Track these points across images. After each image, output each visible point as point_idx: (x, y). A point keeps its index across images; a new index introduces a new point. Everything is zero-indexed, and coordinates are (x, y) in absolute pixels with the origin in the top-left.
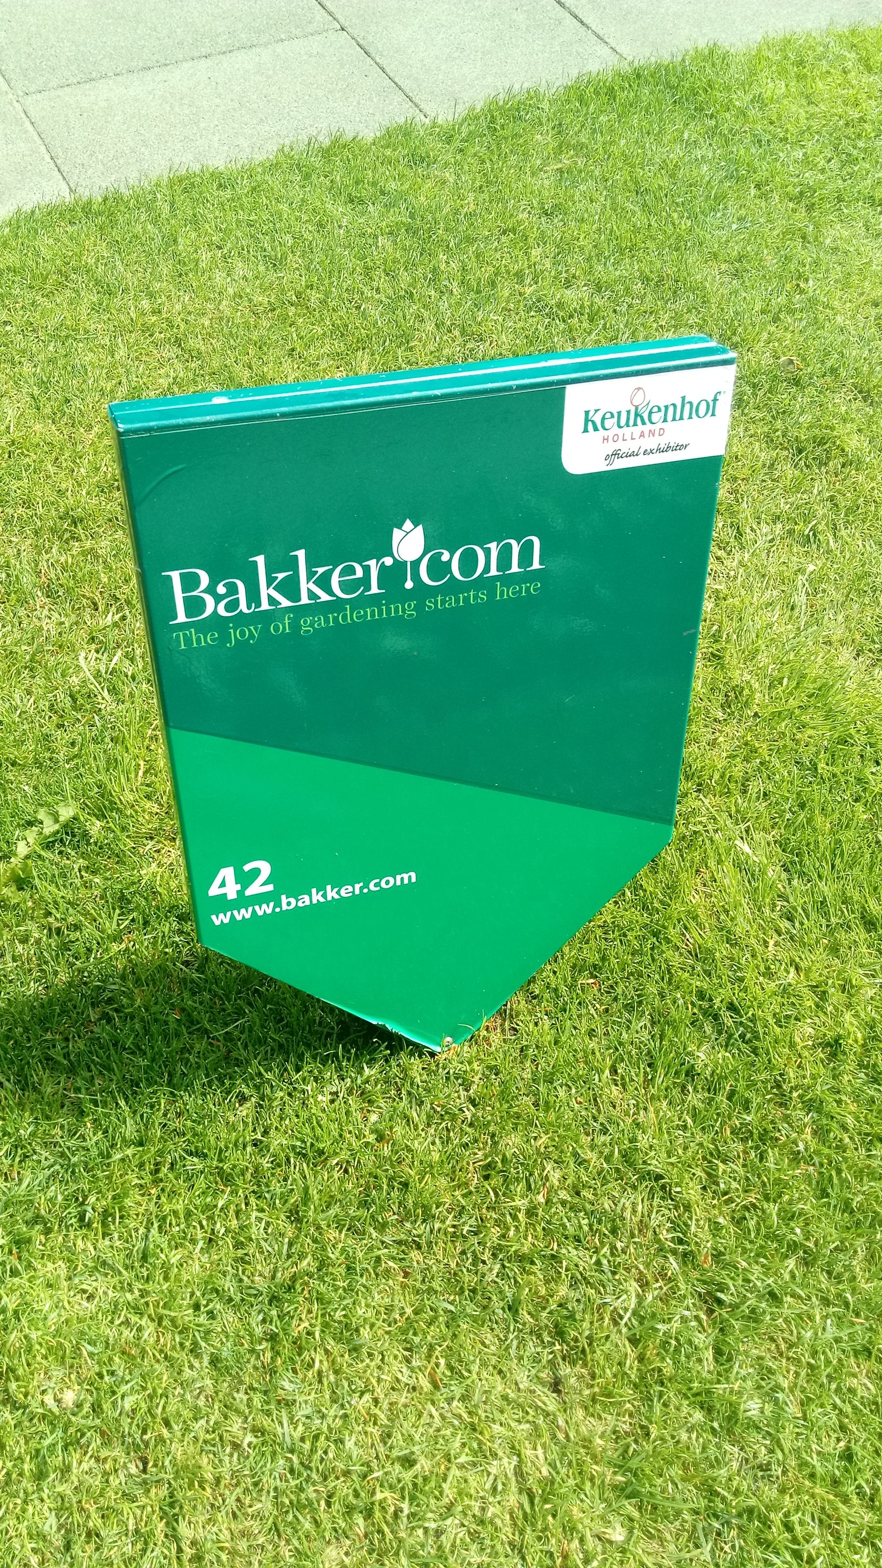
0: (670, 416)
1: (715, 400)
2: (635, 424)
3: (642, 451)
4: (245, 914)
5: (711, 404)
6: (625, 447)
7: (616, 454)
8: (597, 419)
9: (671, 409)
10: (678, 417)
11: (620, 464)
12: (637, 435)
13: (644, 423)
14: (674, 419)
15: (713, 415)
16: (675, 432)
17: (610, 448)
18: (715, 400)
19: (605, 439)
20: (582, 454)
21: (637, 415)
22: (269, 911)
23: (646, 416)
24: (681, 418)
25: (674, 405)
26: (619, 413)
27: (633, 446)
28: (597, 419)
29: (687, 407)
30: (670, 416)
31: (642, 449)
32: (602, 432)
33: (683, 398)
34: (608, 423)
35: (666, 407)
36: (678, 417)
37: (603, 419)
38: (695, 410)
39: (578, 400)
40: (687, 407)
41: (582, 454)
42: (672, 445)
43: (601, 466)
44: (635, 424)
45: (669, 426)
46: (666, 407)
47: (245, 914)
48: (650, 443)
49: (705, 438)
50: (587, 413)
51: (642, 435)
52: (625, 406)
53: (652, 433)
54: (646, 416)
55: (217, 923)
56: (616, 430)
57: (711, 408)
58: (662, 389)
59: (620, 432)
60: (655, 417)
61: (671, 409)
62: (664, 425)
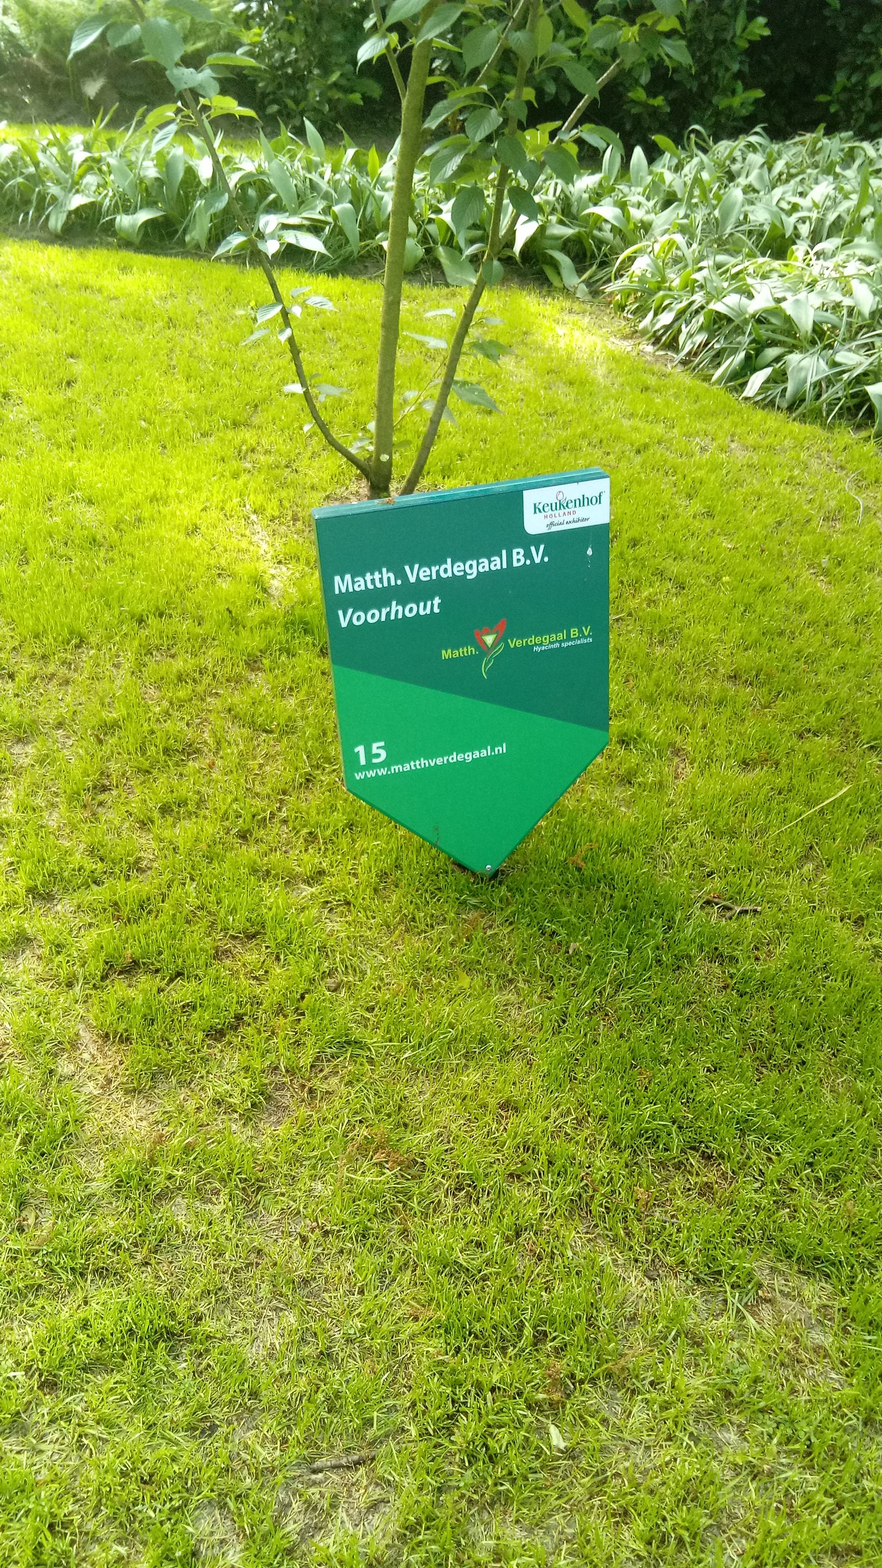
4: (371, 774)
6: (556, 520)
16: (581, 512)
17: (548, 521)
20: (534, 524)
27: (561, 520)
31: (565, 521)
38: (590, 501)
39: (530, 498)
41: (534, 524)
43: (545, 530)
45: (578, 509)
47: (371, 774)
48: (569, 518)
57: (599, 500)
58: (572, 491)
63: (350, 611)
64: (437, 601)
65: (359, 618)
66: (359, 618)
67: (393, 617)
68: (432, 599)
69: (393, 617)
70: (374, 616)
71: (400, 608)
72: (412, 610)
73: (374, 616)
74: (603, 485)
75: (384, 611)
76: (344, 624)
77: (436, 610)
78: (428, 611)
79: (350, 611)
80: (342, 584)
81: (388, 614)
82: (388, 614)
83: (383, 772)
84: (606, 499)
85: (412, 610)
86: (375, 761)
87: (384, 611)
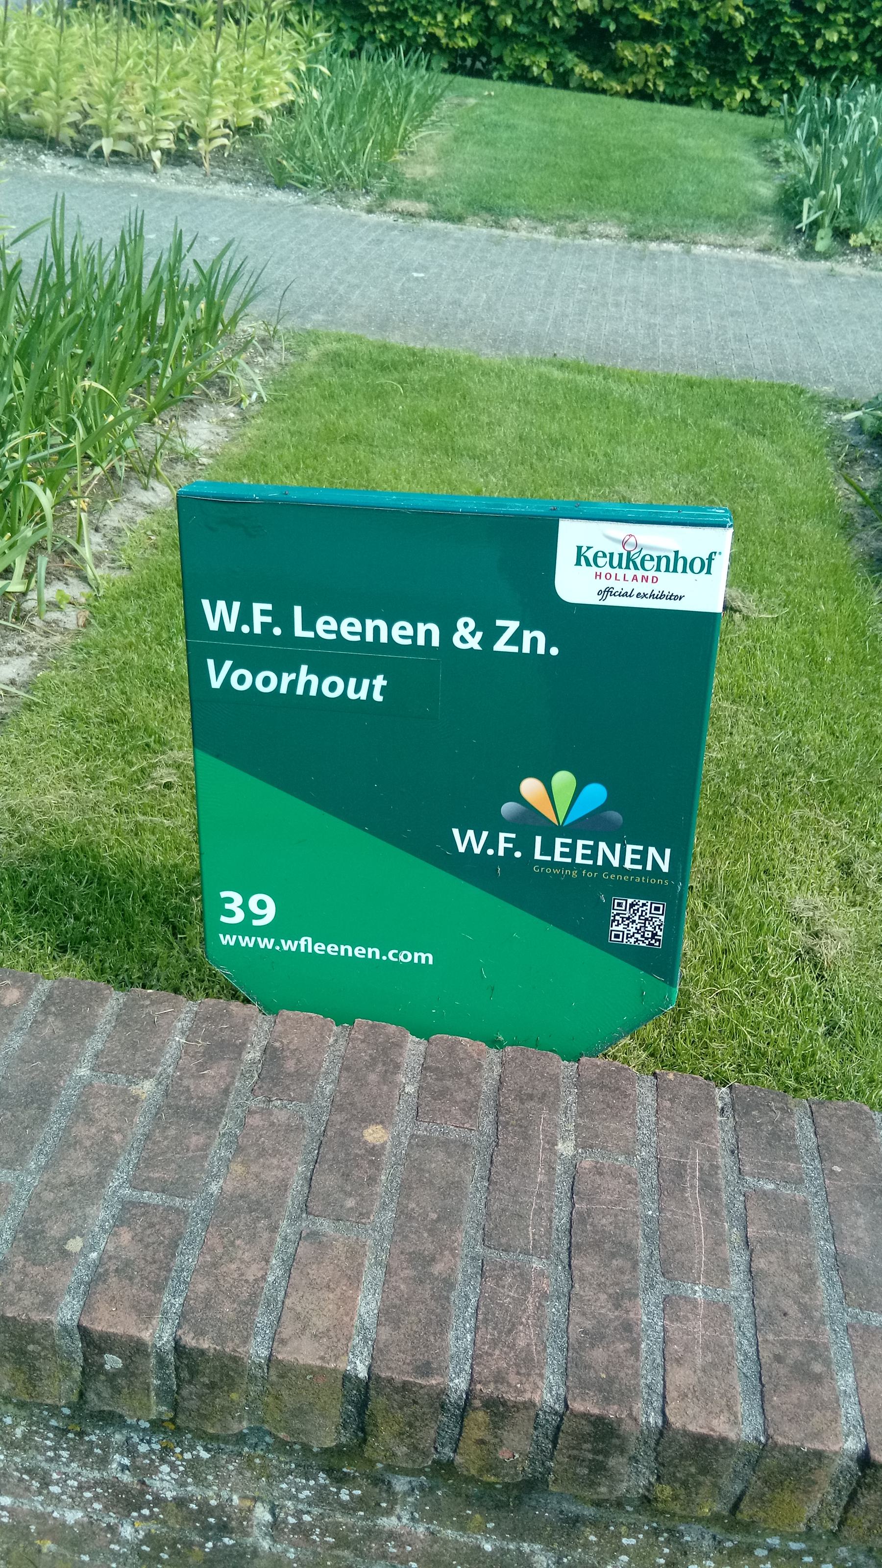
0: (663, 566)
1: (710, 559)
2: (628, 567)
3: (635, 593)
4: (247, 942)
5: (706, 562)
6: (618, 586)
7: (608, 592)
8: (590, 555)
9: (664, 562)
10: (671, 569)
11: (611, 601)
12: (629, 577)
13: (636, 568)
14: (667, 570)
15: (709, 572)
16: (668, 582)
17: (603, 584)
18: (710, 559)
19: (598, 576)
20: (575, 585)
21: (629, 559)
22: (270, 947)
23: (638, 561)
24: (675, 570)
25: (668, 558)
26: (612, 555)
28: (590, 555)
29: (681, 563)
30: (663, 566)
31: (634, 592)
32: (594, 569)
33: (677, 553)
34: (601, 561)
35: (659, 558)
36: (671, 569)
37: (595, 557)
38: (689, 566)
39: (571, 534)
40: (681, 563)
41: (575, 585)
42: (666, 593)
43: (594, 600)
44: (628, 567)
46: (659, 558)
47: (247, 942)
48: (646, 588)
49: (704, 594)
50: (579, 548)
51: (635, 578)
52: (617, 549)
53: (645, 579)
54: (638, 561)
55: (224, 943)
56: (608, 569)
57: (707, 566)
59: (613, 572)
60: (648, 565)
61: (664, 562)
62: (657, 574)
63: (228, 664)
64: (380, 681)
65: (241, 680)
66: (243, 680)
67: (300, 691)
68: (372, 677)
69: (300, 691)
70: (269, 682)
71: (314, 679)
72: (334, 687)
73: (269, 682)
74: (719, 541)
75: (287, 678)
76: (216, 684)
77: (378, 697)
78: (363, 695)
79: (228, 664)
80: (220, 616)
81: (293, 684)
82: (293, 684)
83: (266, 943)
84: (721, 565)
85: (334, 687)
86: (256, 923)
87: (287, 678)
